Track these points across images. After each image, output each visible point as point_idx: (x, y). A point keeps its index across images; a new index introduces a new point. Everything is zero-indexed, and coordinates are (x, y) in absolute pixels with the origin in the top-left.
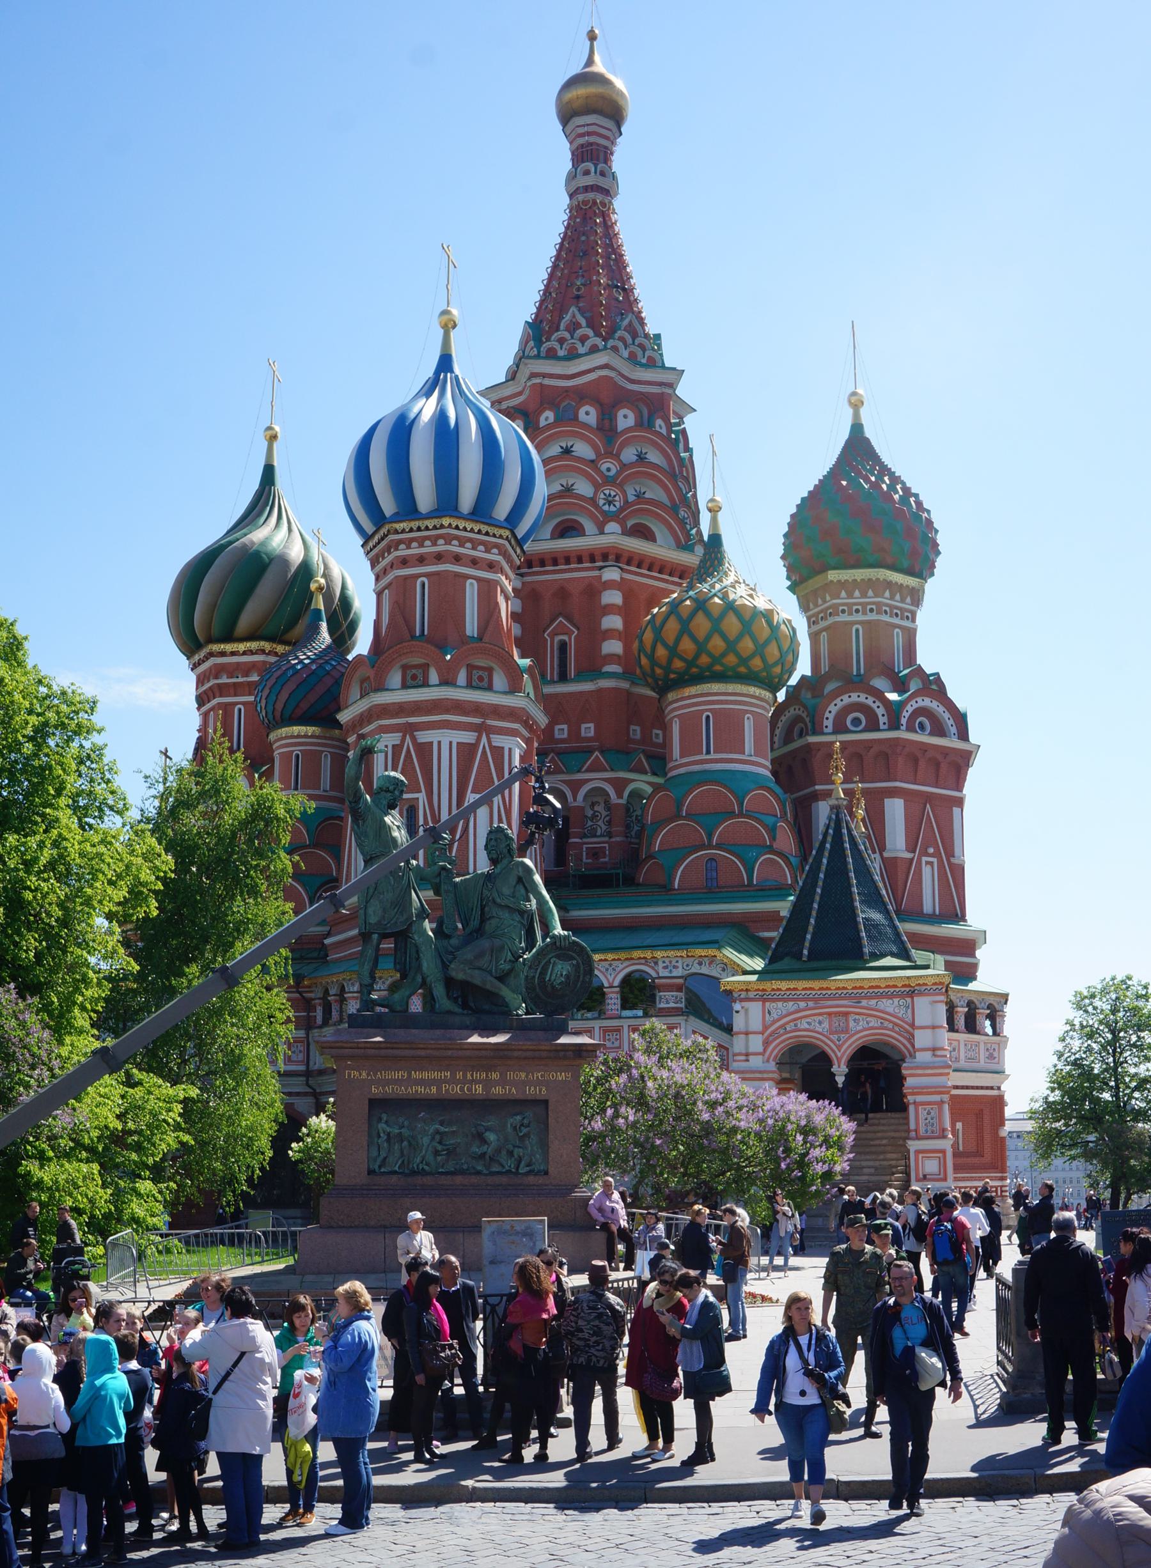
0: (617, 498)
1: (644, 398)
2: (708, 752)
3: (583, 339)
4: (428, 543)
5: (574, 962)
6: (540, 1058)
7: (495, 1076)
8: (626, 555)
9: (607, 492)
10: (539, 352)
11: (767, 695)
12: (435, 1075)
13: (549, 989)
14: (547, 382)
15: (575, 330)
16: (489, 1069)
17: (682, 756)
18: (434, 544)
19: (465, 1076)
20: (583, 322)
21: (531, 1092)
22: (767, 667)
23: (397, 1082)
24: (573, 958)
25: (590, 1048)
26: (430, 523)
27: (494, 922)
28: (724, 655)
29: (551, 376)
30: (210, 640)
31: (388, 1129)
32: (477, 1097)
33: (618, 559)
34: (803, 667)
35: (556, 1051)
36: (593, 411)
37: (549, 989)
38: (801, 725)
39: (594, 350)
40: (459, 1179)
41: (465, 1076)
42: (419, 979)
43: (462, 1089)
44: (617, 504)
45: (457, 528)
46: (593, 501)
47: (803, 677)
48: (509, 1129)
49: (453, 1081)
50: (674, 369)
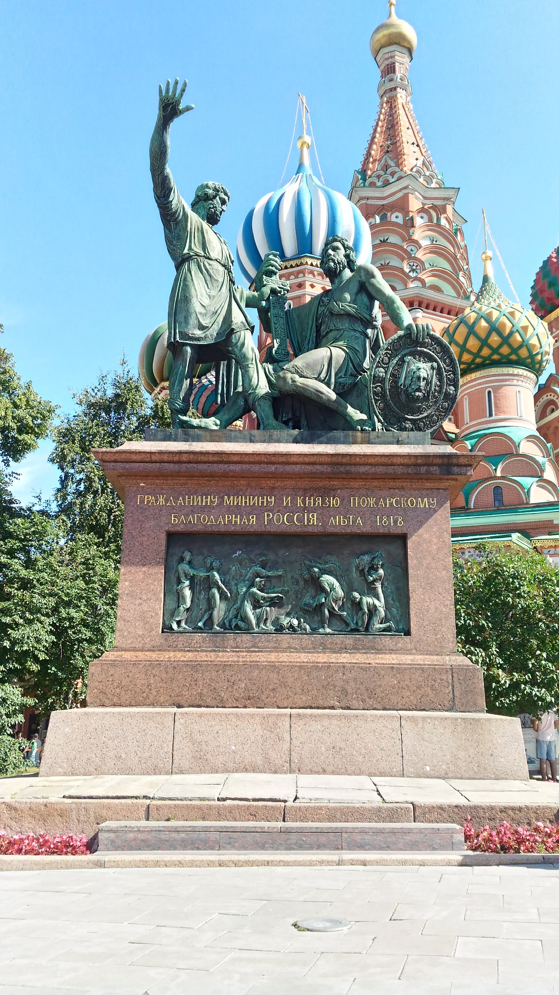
0: (418, 267)
1: (434, 207)
2: (491, 415)
3: (393, 174)
4: (292, 277)
5: (435, 364)
6: (395, 478)
7: (334, 502)
8: (425, 302)
9: (412, 264)
10: (364, 185)
11: (532, 376)
12: (256, 501)
13: (403, 397)
14: (370, 202)
15: (387, 170)
16: (326, 492)
17: (471, 421)
18: (297, 277)
19: (294, 501)
20: (392, 163)
21: (384, 523)
22: (532, 356)
23: (203, 509)
24: (431, 359)
25: (462, 461)
26: (293, 263)
27: (331, 335)
28: (500, 346)
29: (372, 198)
30: (163, 380)
31: (192, 572)
32: (310, 529)
33: (420, 305)
34: (550, 369)
35: (416, 465)
36: (400, 215)
37: (403, 397)
38: (553, 407)
39: (400, 178)
40: (285, 639)
41: (294, 501)
42: (241, 402)
43: (290, 519)
44: (418, 271)
45: (312, 265)
46: (402, 270)
47: (551, 375)
48: (355, 574)
49: (279, 508)
50: (454, 188)
